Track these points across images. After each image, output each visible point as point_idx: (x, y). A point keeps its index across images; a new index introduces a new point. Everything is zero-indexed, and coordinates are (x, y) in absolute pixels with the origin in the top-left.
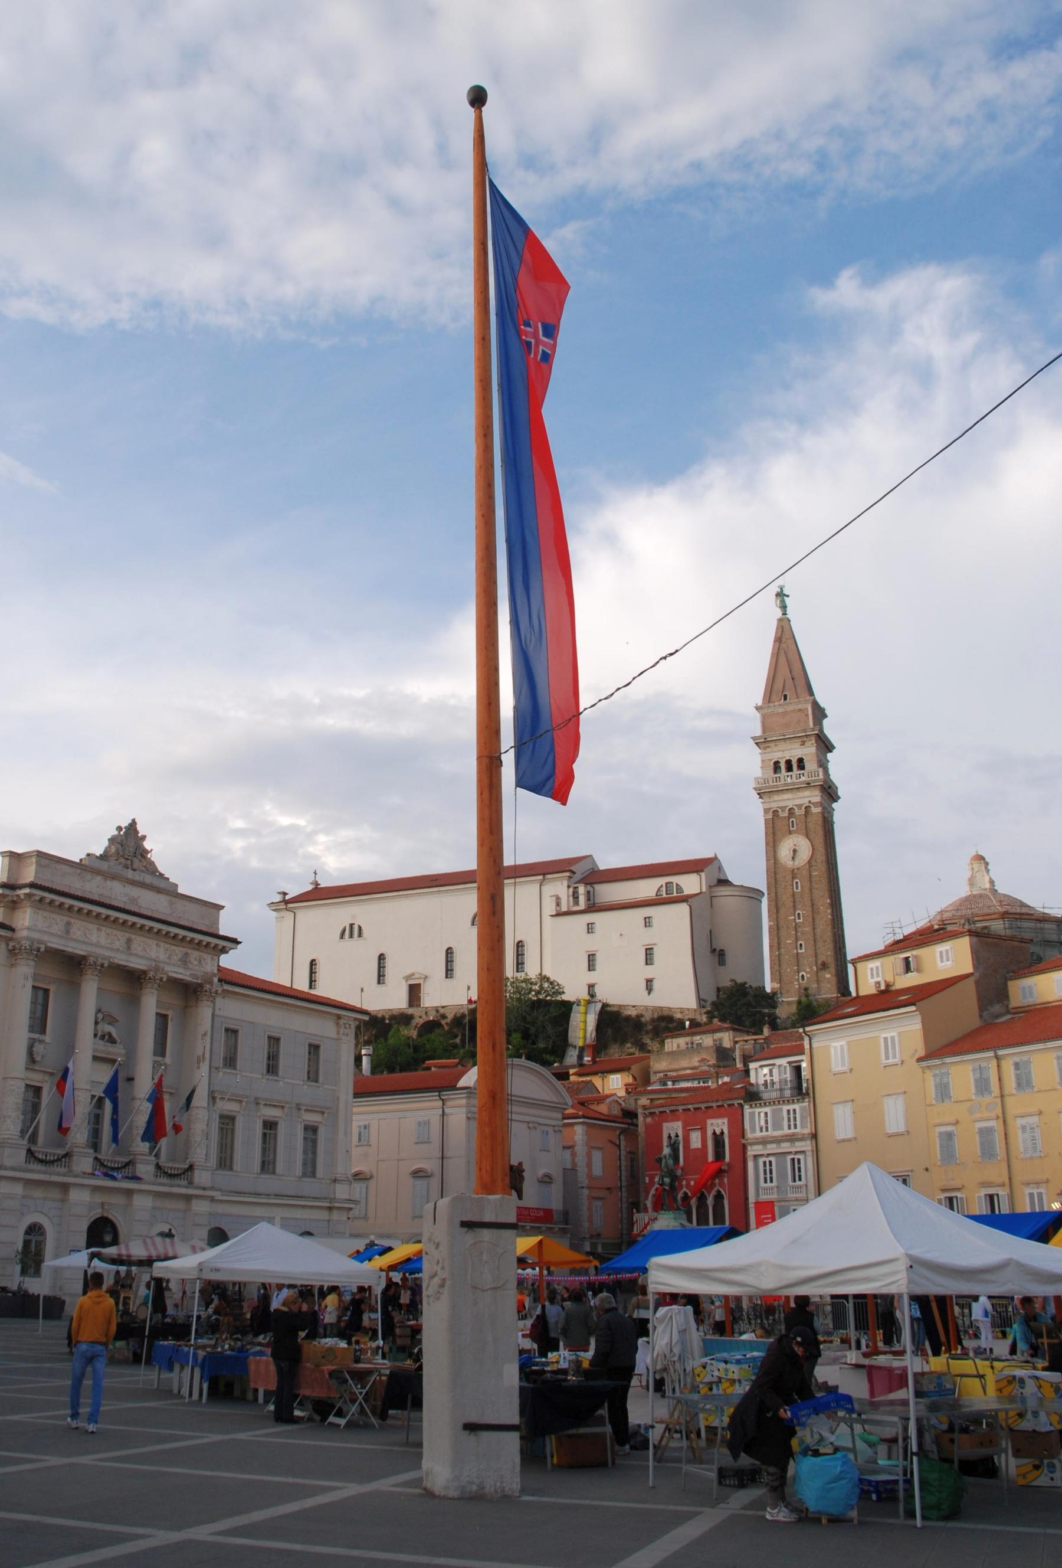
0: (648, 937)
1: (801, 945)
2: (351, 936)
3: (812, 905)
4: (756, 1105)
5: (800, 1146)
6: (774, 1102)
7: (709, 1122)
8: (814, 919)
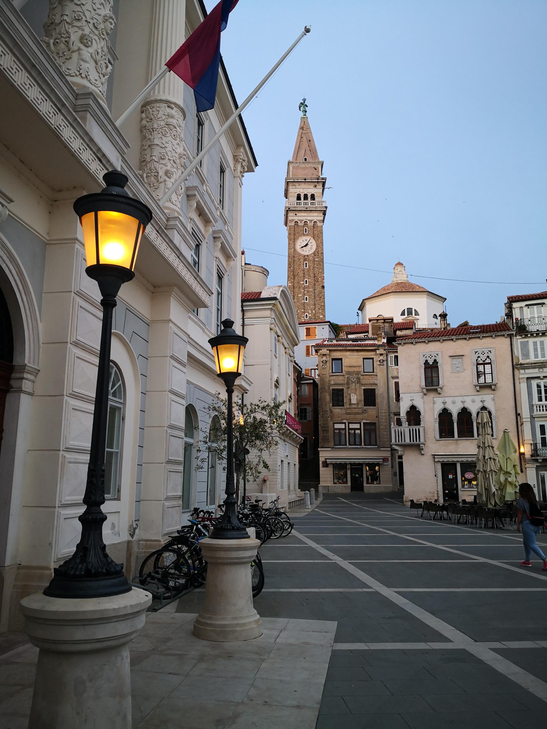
1: (306, 298)
3: (315, 277)
8: (315, 284)
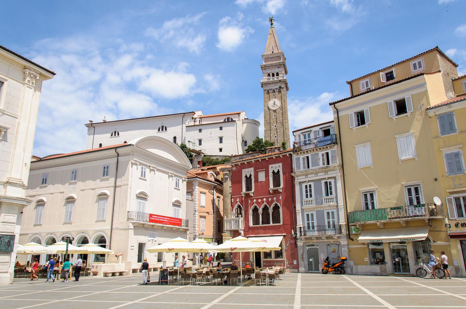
0: (220, 133)
1: (276, 136)
2: (115, 135)
4: (301, 153)
5: (331, 174)
6: (313, 150)
7: (270, 166)
